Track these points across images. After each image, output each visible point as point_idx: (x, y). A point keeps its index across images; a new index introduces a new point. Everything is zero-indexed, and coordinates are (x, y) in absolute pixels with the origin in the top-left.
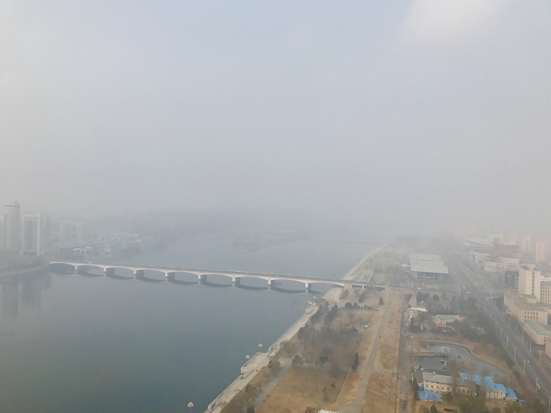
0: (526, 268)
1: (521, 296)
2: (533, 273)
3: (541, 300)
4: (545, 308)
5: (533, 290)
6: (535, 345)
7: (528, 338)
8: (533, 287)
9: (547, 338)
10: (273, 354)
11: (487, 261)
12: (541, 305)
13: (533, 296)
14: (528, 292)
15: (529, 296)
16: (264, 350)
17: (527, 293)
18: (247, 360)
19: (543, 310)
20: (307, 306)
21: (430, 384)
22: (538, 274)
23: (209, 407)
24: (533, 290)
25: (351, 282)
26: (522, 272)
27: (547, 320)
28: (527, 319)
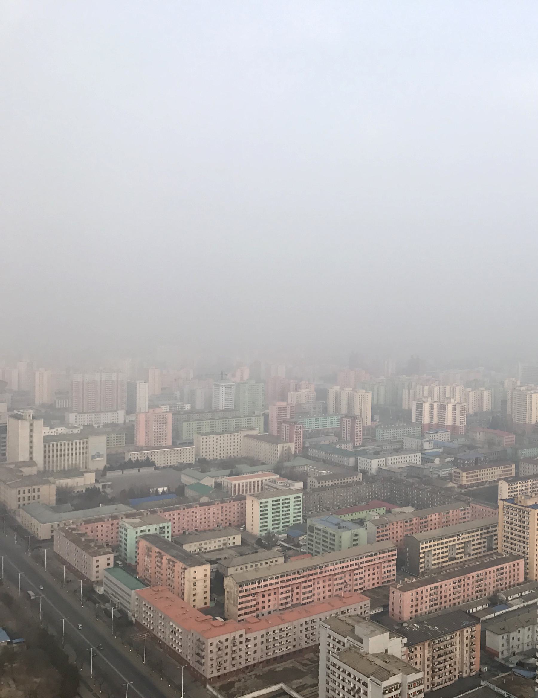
0: (18, 417)
1: (12, 466)
3: (45, 467)
4: (51, 479)
5: (31, 453)
6: (37, 544)
7: (24, 534)
8: (31, 447)
9: (55, 526)
12: (44, 476)
13: (31, 463)
14: (23, 456)
15: (25, 464)
17: (21, 459)
19: (48, 483)
22: (39, 424)
24: (31, 453)
26: (11, 423)
27: (54, 498)
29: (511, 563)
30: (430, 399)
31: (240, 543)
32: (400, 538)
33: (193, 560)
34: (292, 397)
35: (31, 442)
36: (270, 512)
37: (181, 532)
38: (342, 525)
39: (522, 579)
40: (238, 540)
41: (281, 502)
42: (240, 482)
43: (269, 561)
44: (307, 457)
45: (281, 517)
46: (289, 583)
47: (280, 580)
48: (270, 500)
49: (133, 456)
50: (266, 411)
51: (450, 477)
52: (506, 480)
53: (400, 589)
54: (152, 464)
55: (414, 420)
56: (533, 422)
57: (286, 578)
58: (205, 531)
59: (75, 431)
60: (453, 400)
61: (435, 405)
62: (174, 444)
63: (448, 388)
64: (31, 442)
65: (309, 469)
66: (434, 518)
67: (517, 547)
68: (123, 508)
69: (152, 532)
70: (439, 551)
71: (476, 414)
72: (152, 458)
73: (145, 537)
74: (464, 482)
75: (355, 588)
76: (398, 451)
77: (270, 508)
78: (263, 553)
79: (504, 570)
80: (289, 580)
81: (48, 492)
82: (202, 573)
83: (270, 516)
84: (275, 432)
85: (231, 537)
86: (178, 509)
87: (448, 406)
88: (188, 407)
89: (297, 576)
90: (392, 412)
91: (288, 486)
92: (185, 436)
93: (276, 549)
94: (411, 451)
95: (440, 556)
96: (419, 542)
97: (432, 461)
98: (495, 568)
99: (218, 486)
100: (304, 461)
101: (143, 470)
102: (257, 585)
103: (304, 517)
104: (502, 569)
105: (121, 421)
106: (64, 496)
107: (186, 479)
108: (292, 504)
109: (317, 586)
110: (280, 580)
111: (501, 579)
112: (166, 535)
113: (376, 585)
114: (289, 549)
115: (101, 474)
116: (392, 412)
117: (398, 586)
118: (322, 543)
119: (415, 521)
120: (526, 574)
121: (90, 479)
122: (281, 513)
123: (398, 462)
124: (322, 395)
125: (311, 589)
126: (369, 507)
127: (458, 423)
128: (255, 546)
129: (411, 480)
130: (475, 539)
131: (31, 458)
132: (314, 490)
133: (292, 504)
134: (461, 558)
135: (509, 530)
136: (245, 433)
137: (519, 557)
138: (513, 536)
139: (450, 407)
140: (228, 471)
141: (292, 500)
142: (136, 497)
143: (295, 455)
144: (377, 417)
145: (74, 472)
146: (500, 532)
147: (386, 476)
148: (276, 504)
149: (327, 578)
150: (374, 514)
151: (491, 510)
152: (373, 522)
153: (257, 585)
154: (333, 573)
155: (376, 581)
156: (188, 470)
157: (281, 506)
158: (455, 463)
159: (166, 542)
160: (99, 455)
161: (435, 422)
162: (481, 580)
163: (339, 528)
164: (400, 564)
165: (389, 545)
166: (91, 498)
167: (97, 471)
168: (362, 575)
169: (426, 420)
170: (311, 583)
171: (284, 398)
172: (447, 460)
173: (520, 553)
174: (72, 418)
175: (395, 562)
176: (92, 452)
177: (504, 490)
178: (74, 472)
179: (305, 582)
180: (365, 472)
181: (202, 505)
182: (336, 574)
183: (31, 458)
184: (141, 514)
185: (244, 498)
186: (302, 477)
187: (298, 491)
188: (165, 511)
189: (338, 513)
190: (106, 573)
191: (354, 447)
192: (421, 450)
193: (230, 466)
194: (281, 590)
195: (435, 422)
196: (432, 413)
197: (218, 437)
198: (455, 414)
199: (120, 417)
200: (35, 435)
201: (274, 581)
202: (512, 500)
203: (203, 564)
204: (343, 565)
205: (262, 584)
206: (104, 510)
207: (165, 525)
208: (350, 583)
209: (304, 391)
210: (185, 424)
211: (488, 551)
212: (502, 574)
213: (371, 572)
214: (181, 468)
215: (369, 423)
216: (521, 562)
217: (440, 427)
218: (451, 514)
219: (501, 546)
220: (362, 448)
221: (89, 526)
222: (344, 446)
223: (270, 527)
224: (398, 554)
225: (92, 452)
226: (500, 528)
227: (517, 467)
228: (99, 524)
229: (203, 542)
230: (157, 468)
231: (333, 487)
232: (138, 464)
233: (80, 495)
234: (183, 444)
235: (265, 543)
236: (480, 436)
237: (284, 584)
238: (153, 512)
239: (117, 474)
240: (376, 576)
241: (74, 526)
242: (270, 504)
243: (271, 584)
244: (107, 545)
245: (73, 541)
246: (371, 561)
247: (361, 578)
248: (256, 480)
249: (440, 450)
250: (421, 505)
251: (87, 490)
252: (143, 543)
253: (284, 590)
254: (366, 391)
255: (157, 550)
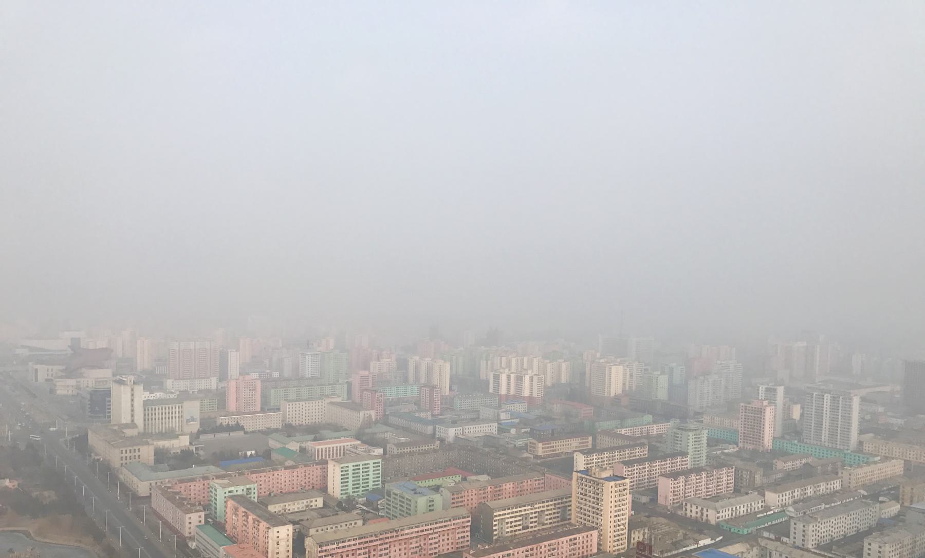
0: (121, 382)
1: (116, 428)
2: (132, 390)
3: (145, 429)
5: (132, 416)
7: (125, 489)
8: (132, 410)
9: (153, 484)
11: (61, 377)
12: (145, 437)
13: (133, 425)
14: (125, 419)
15: (127, 426)
17: (124, 421)
19: (148, 444)
22: (139, 389)
24: (132, 416)
26: (114, 388)
28: (124, 462)
29: (585, 534)
30: (507, 370)
31: (321, 505)
32: (474, 505)
33: (276, 520)
34: (374, 366)
35: (132, 405)
36: (350, 476)
37: (267, 493)
38: (418, 490)
39: (595, 550)
40: (320, 502)
41: (361, 467)
42: (323, 447)
43: (348, 524)
44: (386, 423)
45: (361, 481)
46: (367, 545)
47: (357, 542)
48: (350, 465)
49: (224, 420)
50: (350, 380)
51: (525, 448)
52: (582, 452)
53: (473, 555)
54: (242, 428)
55: (491, 391)
56: (612, 395)
57: (363, 540)
58: (289, 493)
59: (172, 396)
60: (530, 372)
61: (512, 376)
62: (263, 410)
63: (525, 359)
64: (132, 405)
65: (388, 436)
66: (508, 487)
67: (591, 518)
68: (213, 469)
69: (240, 493)
70: (513, 519)
71: (553, 386)
72: (242, 423)
73: (233, 498)
74: (540, 453)
75: (430, 552)
76: (476, 420)
77: (350, 472)
78: (343, 516)
79: (577, 541)
80: (367, 542)
81: (147, 453)
82: (285, 532)
83: (351, 480)
84: (358, 400)
85: (314, 500)
86: (264, 471)
87: (525, 377)
88: (276, 375)
89: (374, 538)
90: (470, 382)
91: (368, 451)
92: (273, 403)
93: (355, 512)
94: (486, 421)
95: (514, 524)
96: (492, 510)
97: (508, 431)
98: (568, 538)
99: (303, 450)
100: (385, 428)
101: (234, 434)
102: (335, 546)
103: (383, 482)
104: (575, 539)
105: (214, 387)
106: (161, 456)
107: (272, 444)
108: (371, 469)
109: (393, 548)
110: (357, 542)
111: (574, 549)
112: (252, 495)
113: (450, 550)
114: (368, 512)
115: (195, 437)
116: (470, 382)
117: (471, 552)
118: (399, 507)
119: (489, 489)
120: (599, 545)
121: (184, 442)
122: (361, 478)
123: (474, 431)
124: (402, 364)
125: (387, 551)
126: (445, 474)
127: (535, 395)
128: (337, 509)
129: (487, 450)
130: (549, 509)
131: (133, 421)
132: (393, 456)
133: (371, 469)
134: (534, 527)
135: (583, 501)
136: (329, 401)
137: (593, 528)
138: (586, 508)
139: (527, 379)
140: (312, 436)
141: (371, 466)
142: (227, 460)
143: (376, 423)
144: (455, 387)
145: (171, 434)
146: (574, 504)
147: (461, 444)
148: (356, 469)
149: (403, 542)
150: (449, 482)
151: (566, 481)
152: (448, 489)
153: (335, 546)
154: (408, 536)
155: (450, 547)
156: (274, 435)
157: (361, 471)
158: (532, 434)
159: (252, 503)
160: (193, 419)
161: (512, 392)
162: (554, 549)
163: (415, 493)
164: (474, 530)
165: (463, 511)
166: (185, 459)
167: (191, 435)
168: (436, 540)
169: (503, 391)
170: (387, 546)
171: (366, 368)
172: (523, 430)
173: (594, 525)
174: (169, 383)
175: (468, 529)
176: (186, 416)
177: (580, 462)
178: (171, 434)
179: (381, 544)
180: (442, 440)
181: (286, 468)
182: (411, 538)
183: (133, 421)
184: (230, 475)
185: (326, 463)
186: (382, 444)
187: (377, 457)
188: (252, 473)
189: (415, 479)
190: (198, 530)
191: (433, 415)
192: (498, 420)
193: (315, 431)
194: (358, 552)
195: (512, 392)
196: (509, 384)
197: (303, 403)
198: (531, 385)
199: (213, 383)
200: (135, 399)
201: (352, 543)
202: (586, 472)
203: (285, 524)
204: (418, 529)
205: (341, 545)
206: (197, 470)
207: (251, 486)
208: (425, 547)
209: (385, 361)
210: (273, 391)
211: (561, 521)
212: (575, 544)
213: (446, 537)
214: (268, 432)
215: (447, 393)
216: (595, 533)
217: (517, 398)
218: (525, 484)
219: (574, 517)
220: (440, 417)
221: (183, 485)
222: (423, 415)
223: (350, 491)
224: (472, 521)
225: (186, 416)
226: (573, 499)
227: (594, 439)
228: (192, 484)
229: (287, 504)
230: (246, 433)
231: (411, 454)
232: (229, 429)
233: (176, 456)
234: (270, 410)
235: (346, 506)
236: (557, 408)
237: (361, 546)
238: (240, 474)
239: (210, 437)
240: (450, 541)
241: (169, 485)
242: (351, 468)
243: (349, 546)
244: (200, 504)
245: (168, 499)
246: (445, 526)
247: (436, 543)
248: (338, 445)
249: (517, 421)
250: (496, 474)
251: (182, 451)
252: (231, 503)
253: (362, 551)
254: (445, 361)
255: (244, 510)
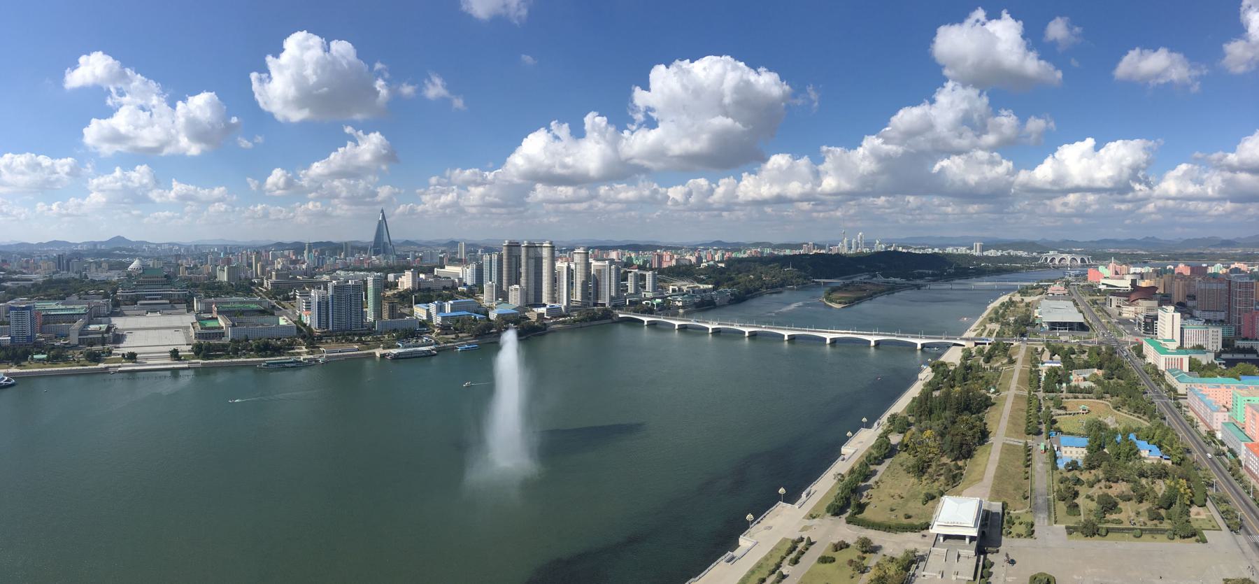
10: (880, 431)
16: (869, 425)
18: (847, 439)
20: (920, 370)
21: (1068, 449)
23: (804, 495)
25: (972, 339)
